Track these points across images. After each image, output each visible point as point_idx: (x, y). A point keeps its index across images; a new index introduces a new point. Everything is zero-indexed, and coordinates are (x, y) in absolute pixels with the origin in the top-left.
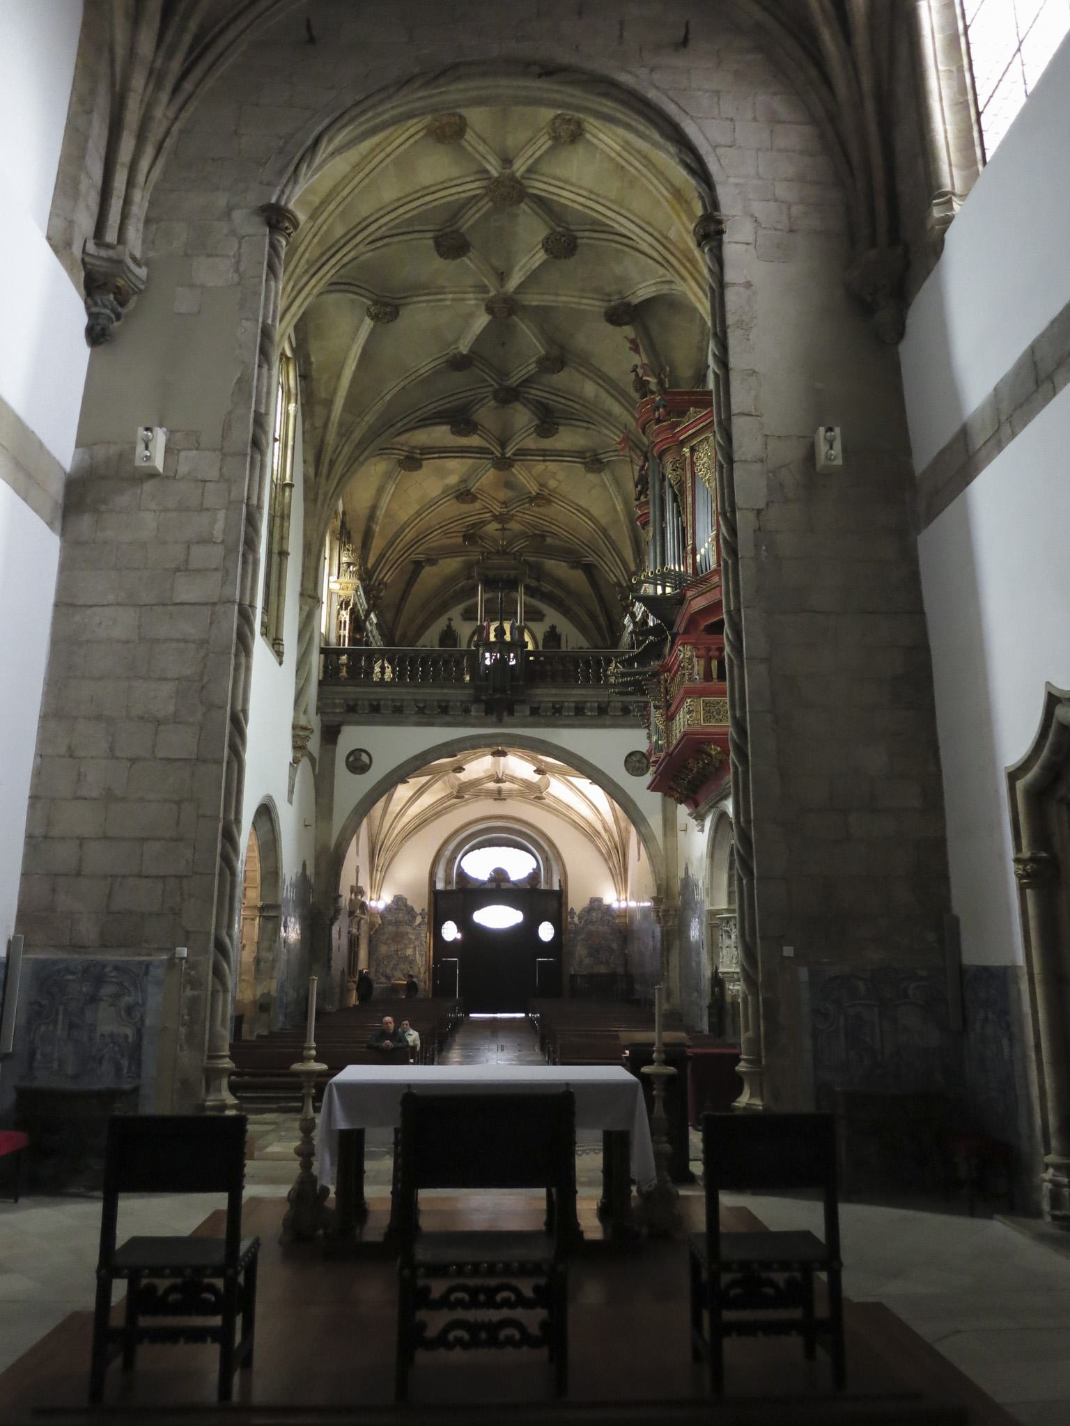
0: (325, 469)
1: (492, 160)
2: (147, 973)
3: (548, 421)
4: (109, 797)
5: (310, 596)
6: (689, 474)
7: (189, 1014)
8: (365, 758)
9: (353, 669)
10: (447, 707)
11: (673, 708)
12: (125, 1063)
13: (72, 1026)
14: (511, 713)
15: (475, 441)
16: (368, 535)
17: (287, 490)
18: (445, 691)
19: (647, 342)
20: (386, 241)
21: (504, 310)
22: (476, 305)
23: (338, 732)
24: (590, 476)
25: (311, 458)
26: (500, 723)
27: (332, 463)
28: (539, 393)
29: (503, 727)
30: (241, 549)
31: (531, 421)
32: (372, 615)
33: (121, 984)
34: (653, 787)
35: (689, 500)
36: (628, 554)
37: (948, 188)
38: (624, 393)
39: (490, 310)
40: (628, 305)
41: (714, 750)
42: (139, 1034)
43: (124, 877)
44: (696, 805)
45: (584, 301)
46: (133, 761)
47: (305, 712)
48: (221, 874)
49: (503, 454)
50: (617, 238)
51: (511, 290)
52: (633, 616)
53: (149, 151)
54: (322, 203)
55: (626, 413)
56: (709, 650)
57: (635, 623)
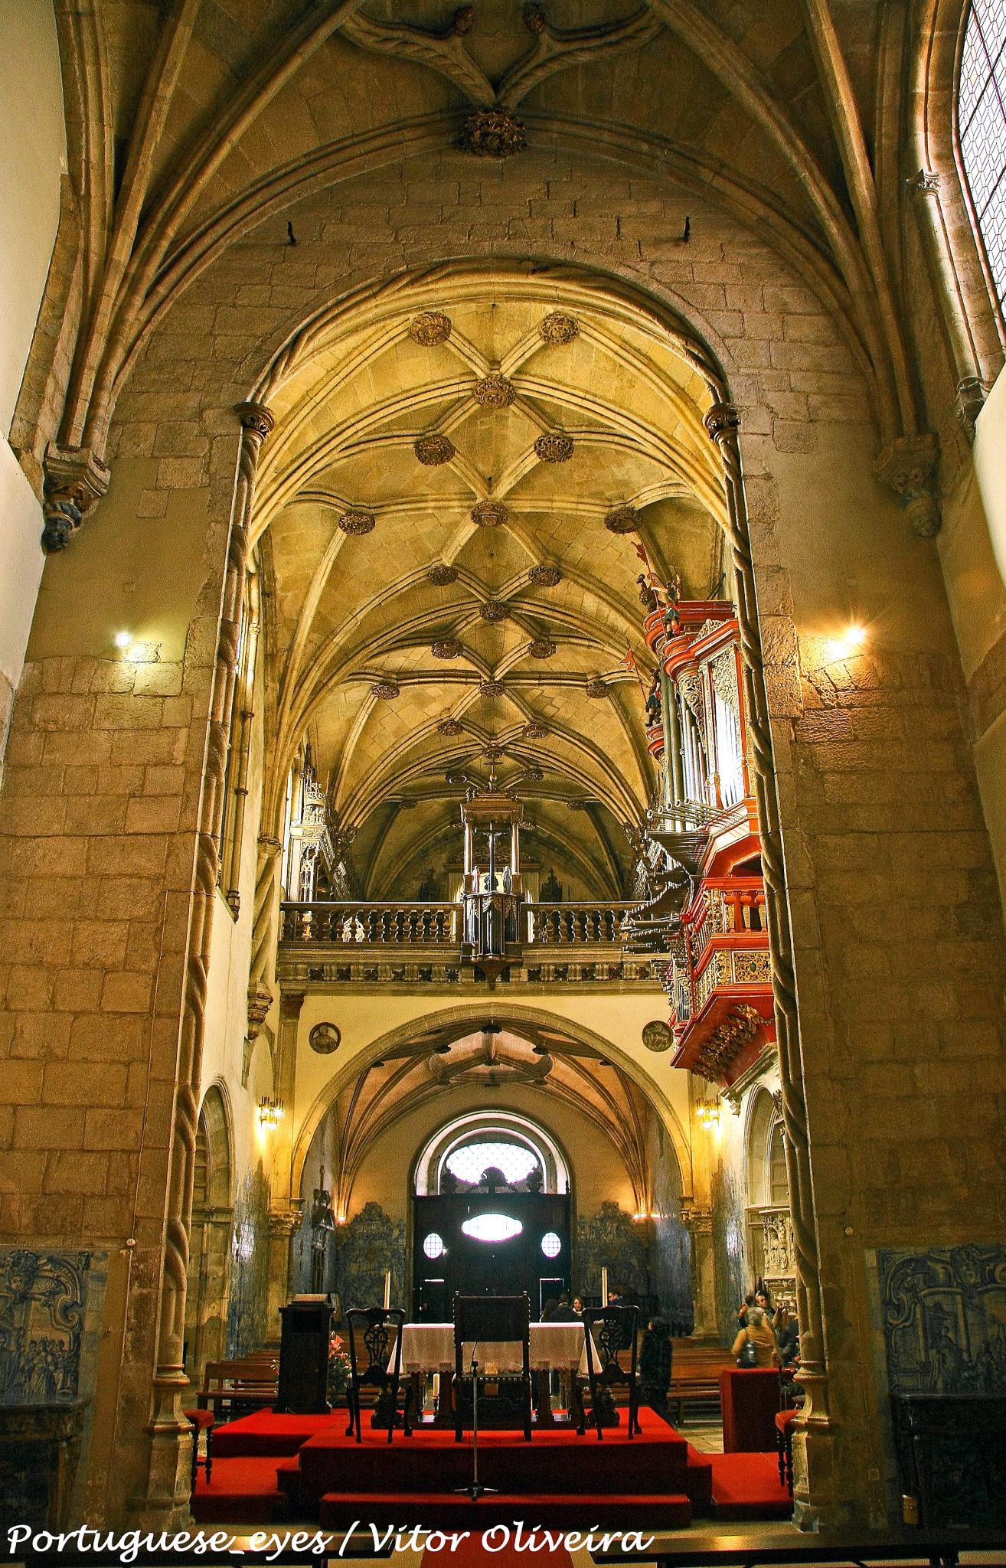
1: (478, 361)
2: (87, 1266)
3: (544, 638)
4: (49, 1057)
6: (707, 693)
7: (137, 1316)
8: (332, 1034)
10: (430, 972)
11: (699, 965)
12: (59, 1376)
14: (506, 978)
15: (460, 663)
16: (336, 773)
18: (427, 953)
19: (651, 549)
20: (362, 446)
21: (492, 518)
22: (463, 514)
23: (301, 1003)
24: (593, 701)
26: (492, 990)
29: (497, 995)
30: (204, 772)
31: (524, 640)
32: (341, 866)
34: (678, 1063)
35: (710, 722)
37: (975, 375)
38: (629, 607)
39: (476, 518)
40: (631, 510)
41: (750, 1012)
42: (77, 1340)
43: (63, 1151)
44: (730, 1081)
45: (581, 507)
46: (76, 1015)
48: (176, 1149)
49: (492, 678)
50: (617, 439)
51: (501, 496)
52: (647, 861)
53: (120, 353)
54: (291, 411)
55: (632, 628)
56: (739, 894)
57: (649, 870)
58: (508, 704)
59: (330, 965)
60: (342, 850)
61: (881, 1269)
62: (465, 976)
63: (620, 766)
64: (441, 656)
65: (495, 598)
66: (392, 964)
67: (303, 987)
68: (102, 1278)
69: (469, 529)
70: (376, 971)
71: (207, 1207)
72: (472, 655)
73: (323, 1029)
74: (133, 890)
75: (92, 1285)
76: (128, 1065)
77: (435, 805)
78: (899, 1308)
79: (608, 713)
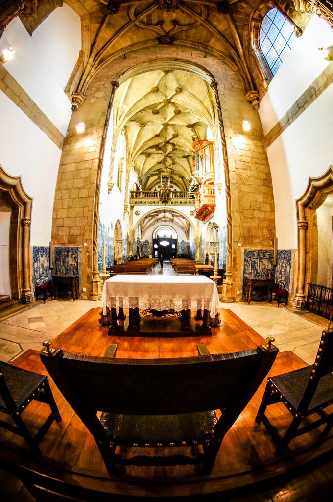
0: (130, 156)
4: (69, 208)
5: (128, 180)
12: (75, 271)
13: (64, 262)
25: (128, 154)
27: (132, 155)
33: (73, 252)
39: (163, 125)
41: (209, 208)
46: (74, 198)
48: (94, 225)
58: (169, 159)
60: (140, 182)
61: (245, 253)
63: (187, 170)
64: (157, 150)
68: (81, 252)
69: (162, 127)
72: (163, 150)
74: (85, 171)
75: (79, 253)
76: (84, 208)
77: (155, 177)
78: (247, 261)
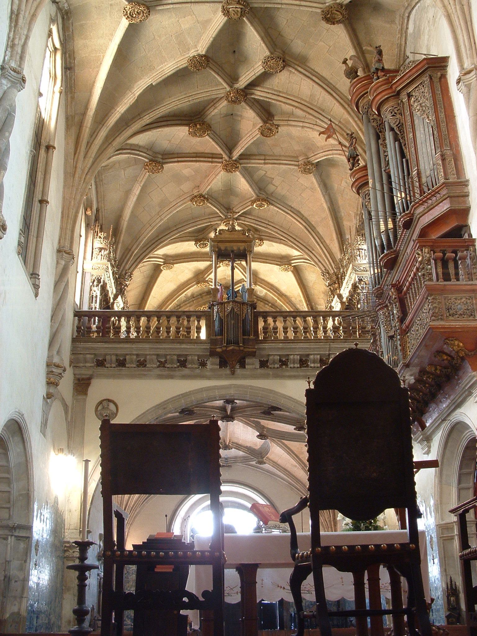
8: (112, 407)
9: (104, 330)
10: (185, 361)
14: (243, 366)
17: (51, 151)
18: (184, 346)
23: (88, 385)
28: (262, 94)
29: (236, 378)
31: (254, 125)
36: (335, 247)
47: (58, 352)
52: (340, 297)
57: (342, 303)
59: (111, 355)
62: (212, 363)
63: (320, 230)
65: (236, 86)
66: (158, 355)
67: (90, 372)
70: (145, 361)
71: (11, 523)
73: (105, 403)
79: (313, 189)
